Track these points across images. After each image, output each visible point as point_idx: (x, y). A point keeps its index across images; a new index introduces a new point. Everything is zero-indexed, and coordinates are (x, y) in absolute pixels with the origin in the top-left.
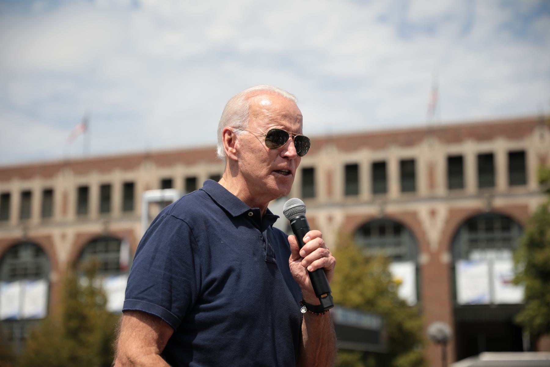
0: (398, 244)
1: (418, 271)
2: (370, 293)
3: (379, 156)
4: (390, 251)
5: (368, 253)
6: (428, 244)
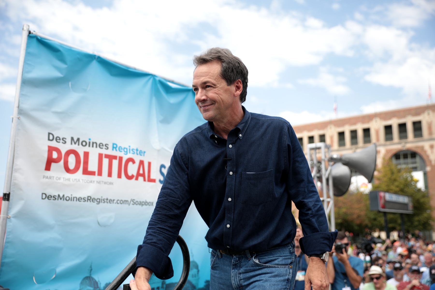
0: (415, 163)
1: (425, 174)
2: (402, 186)
3: (402, 121)
5: (399, 167)
6: (430, 161)
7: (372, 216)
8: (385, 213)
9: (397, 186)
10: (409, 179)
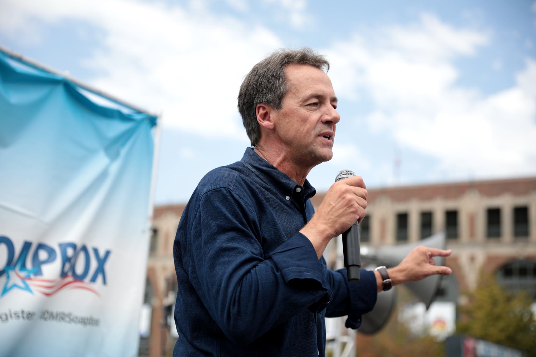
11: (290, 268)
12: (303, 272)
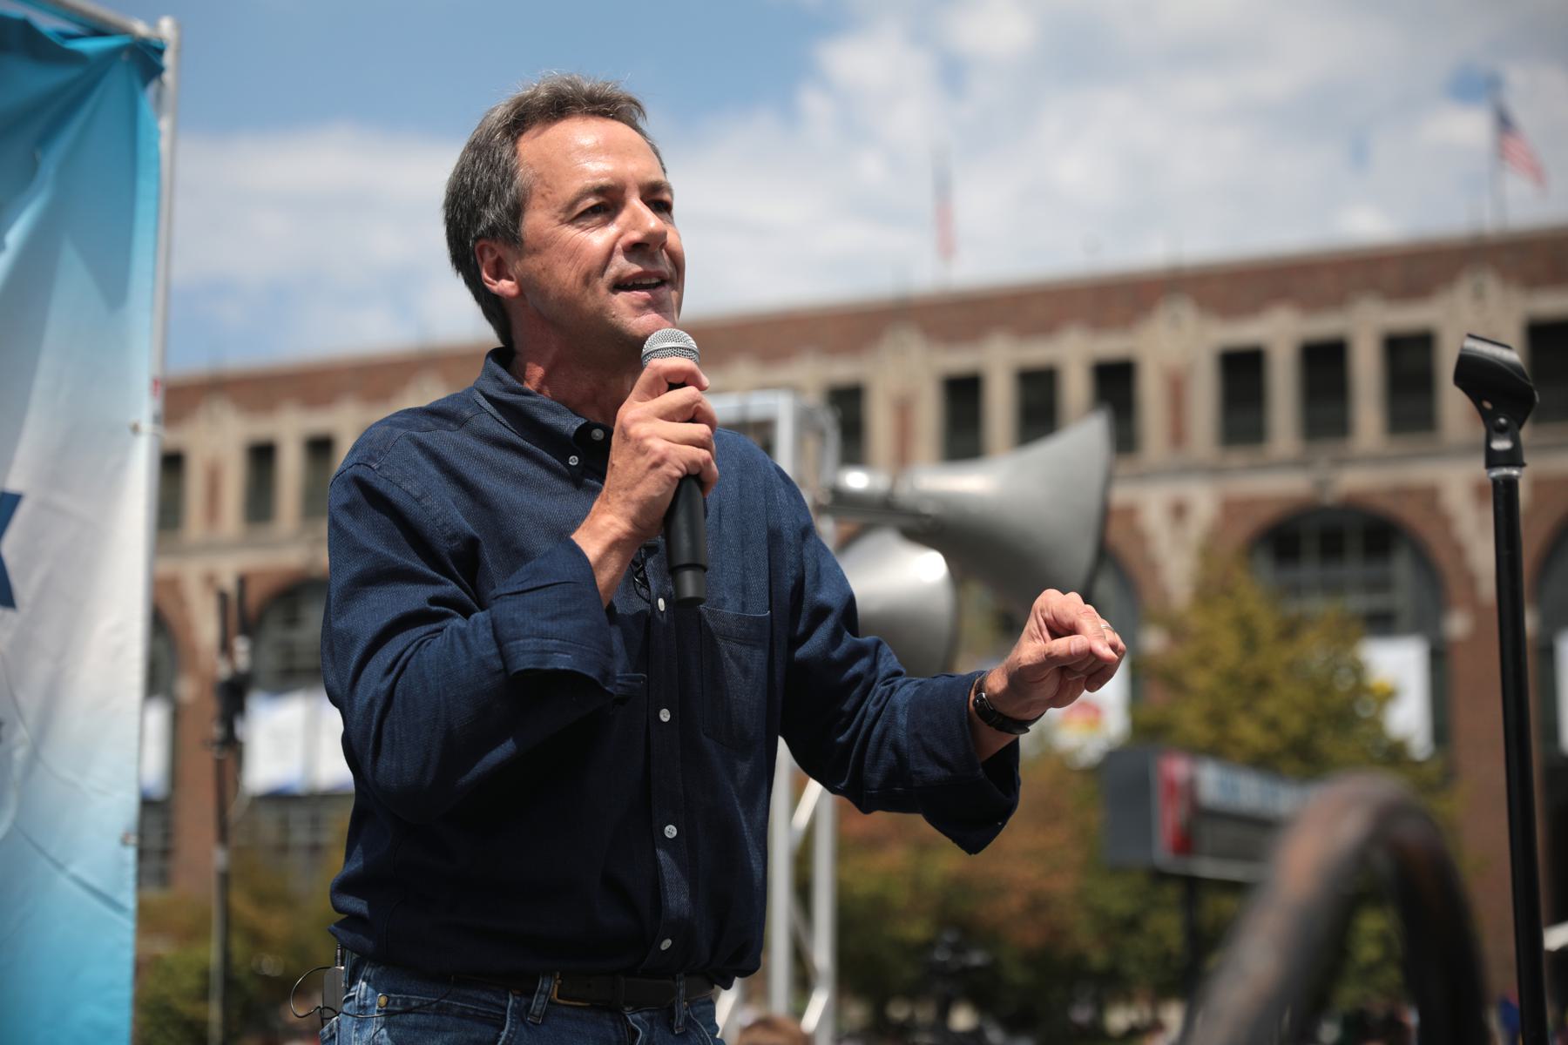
1: (1440, 660)
2: (1294, 724)
3: (1323, 326)
4: (1357, 603)
5: (1293, 608)
7: (1117, 899)
8: (1193, 886)
9: (1272, 725)
10: (1344, 684)
11: (521, 642)
12: (552, 652)
